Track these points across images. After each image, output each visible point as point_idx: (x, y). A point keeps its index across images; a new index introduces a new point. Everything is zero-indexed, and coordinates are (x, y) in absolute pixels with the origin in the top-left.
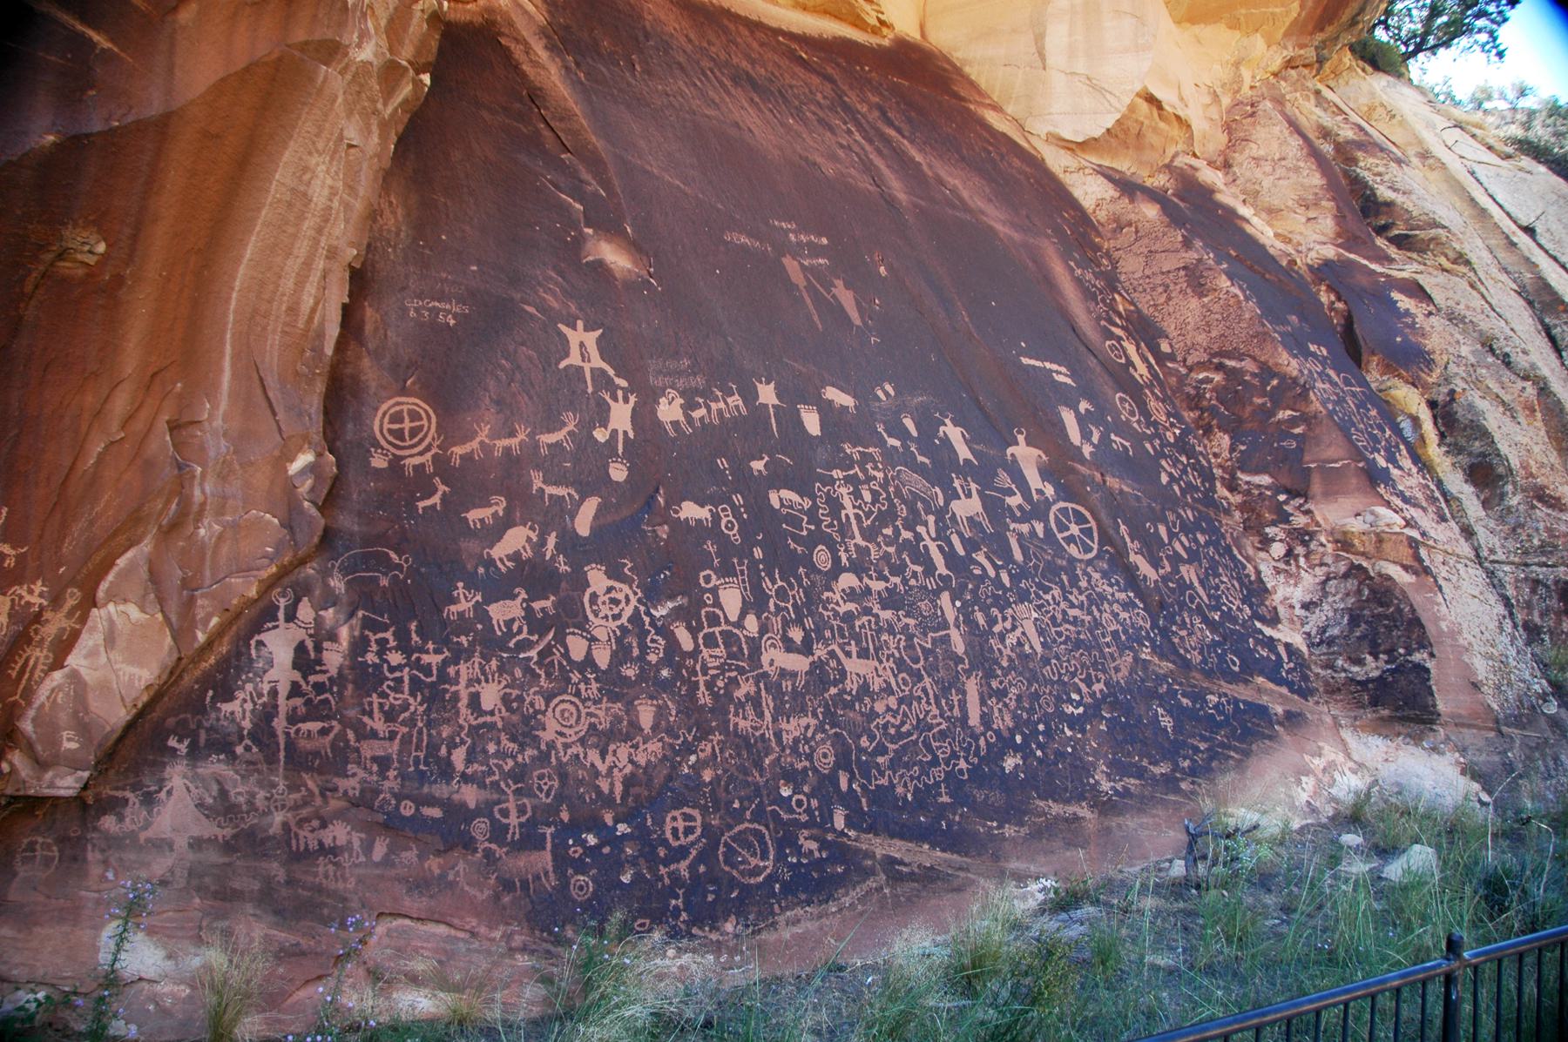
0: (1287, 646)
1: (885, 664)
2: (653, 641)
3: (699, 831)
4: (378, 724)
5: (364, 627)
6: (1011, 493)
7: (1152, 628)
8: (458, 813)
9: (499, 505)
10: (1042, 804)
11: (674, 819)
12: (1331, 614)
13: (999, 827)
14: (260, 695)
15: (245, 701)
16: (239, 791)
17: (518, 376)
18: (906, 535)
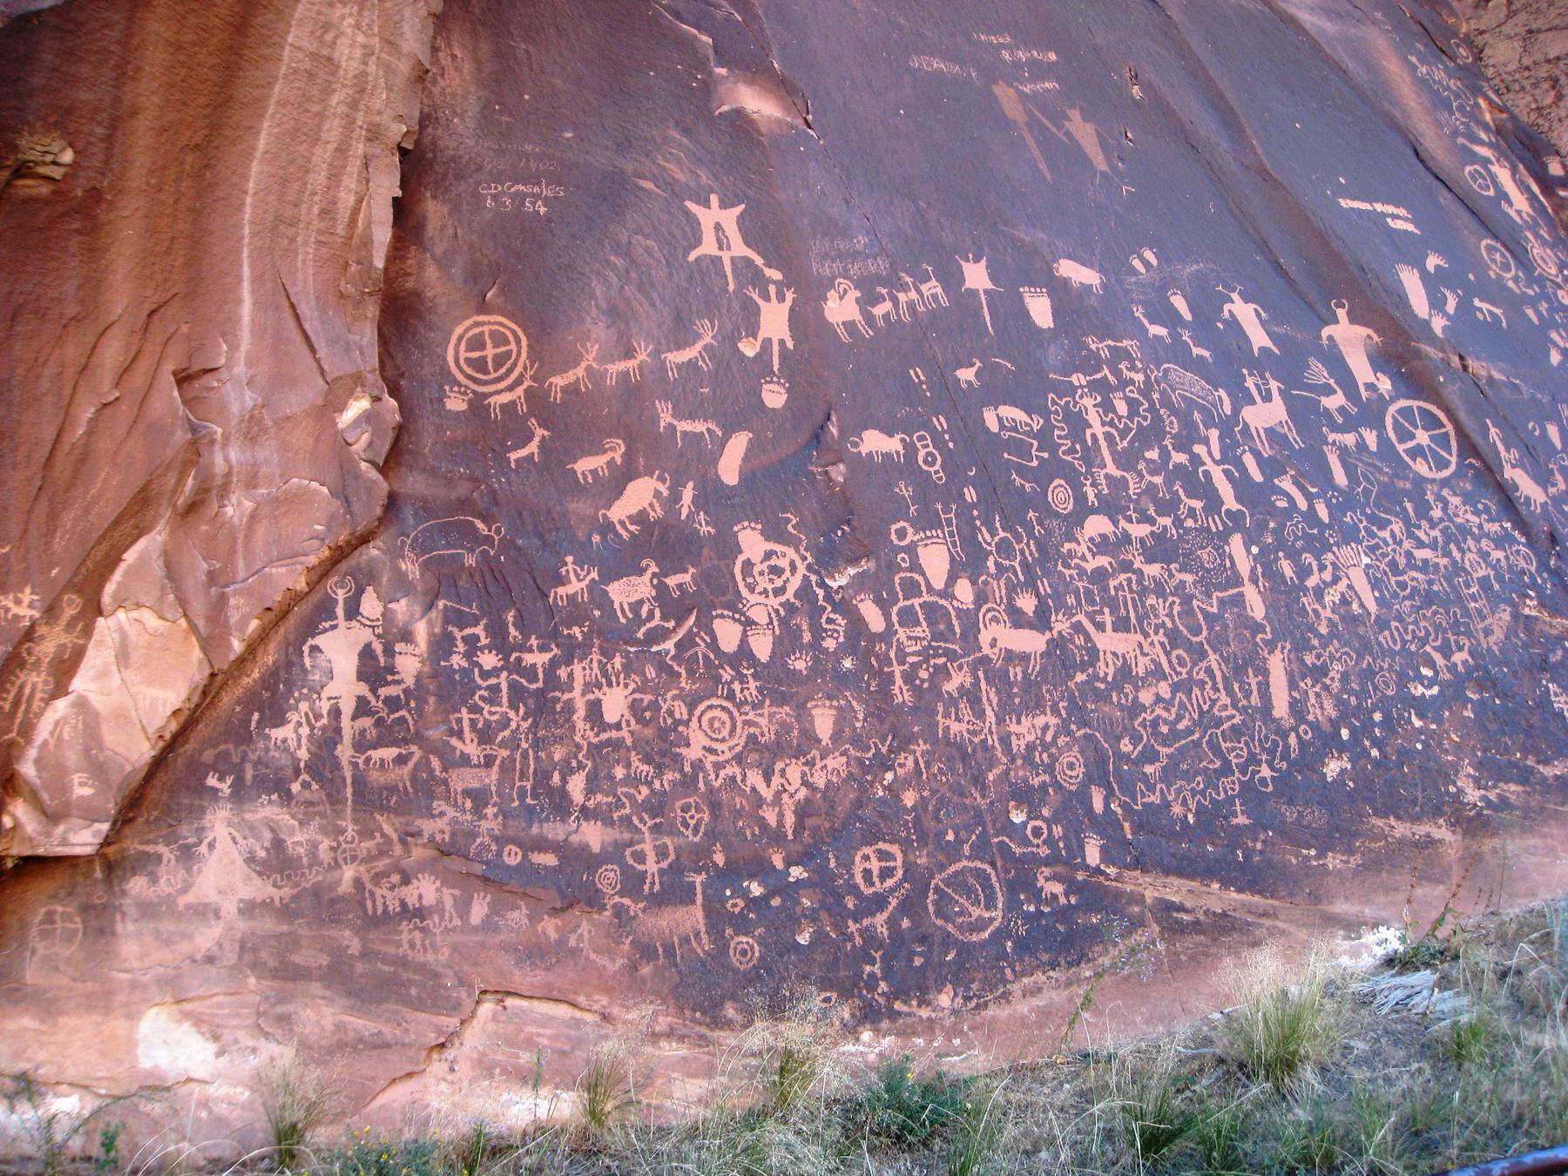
1: (1155, 639)
2: (829, 621)
3: (900, 873)
4: (472, 749)
5: (447, 620)
6: (1329, 391)
8: (577, 859)
9: (616, 451)
10: (1380, 822)
11: (866, 858)
13: (1318, 857)
14: (318, 716)
15: (299, 724)
16: (298, 839)
17: (634, 275)
18: (1179, 458)
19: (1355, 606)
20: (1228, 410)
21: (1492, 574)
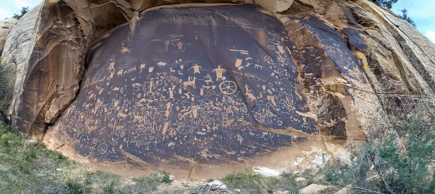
0: (308, 119)
10: (177, 156)
12: (324, 108)
18: (164, 90)
19: (191, 116)
20: (180, 82)
21: (233, 112)
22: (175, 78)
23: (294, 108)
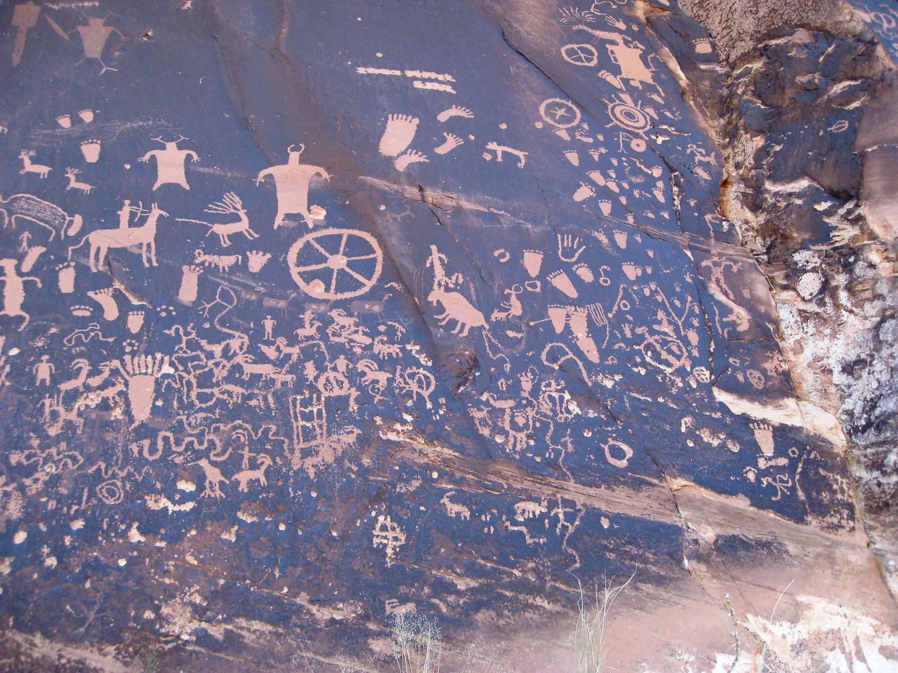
6: (236, 218)
7: (433, 397)
12: (885, 377)
20: (72, 232)
21: (354, 393)
22: (46, 210)
23: (705, 375)
